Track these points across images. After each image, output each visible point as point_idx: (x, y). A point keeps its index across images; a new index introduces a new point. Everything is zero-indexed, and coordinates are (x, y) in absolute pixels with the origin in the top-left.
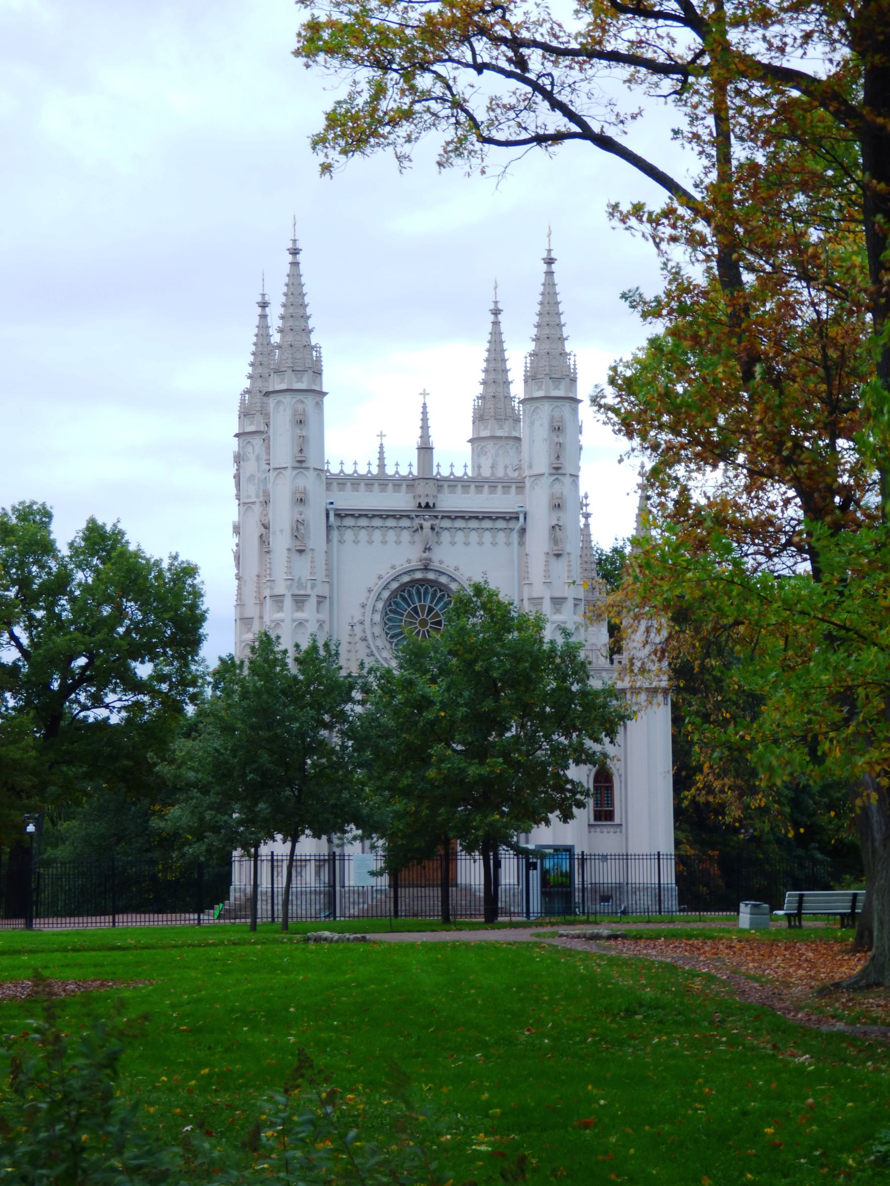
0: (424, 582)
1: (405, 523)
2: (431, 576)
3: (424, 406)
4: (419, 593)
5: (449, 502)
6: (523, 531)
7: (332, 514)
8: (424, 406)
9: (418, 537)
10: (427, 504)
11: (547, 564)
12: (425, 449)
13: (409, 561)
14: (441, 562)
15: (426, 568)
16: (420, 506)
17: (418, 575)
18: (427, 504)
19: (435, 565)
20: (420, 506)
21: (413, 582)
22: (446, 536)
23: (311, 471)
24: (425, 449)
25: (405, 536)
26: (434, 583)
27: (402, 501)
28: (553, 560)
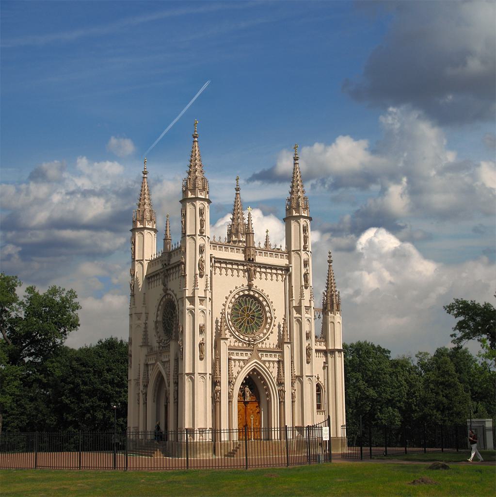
0: (248, 295)
1: (241, 267)
2: (252, 293)
4: (246, 301)
5: (259, 259)
6: (290, 276)
7: (213, 259)
14: (256, 287)
15: (249, 290)
16: (249, 260)
17: (246, 293)
19: (254, 288)
20: (249, 260)
21: (244, 295)
26: (253, 297)
27: (240, 257)
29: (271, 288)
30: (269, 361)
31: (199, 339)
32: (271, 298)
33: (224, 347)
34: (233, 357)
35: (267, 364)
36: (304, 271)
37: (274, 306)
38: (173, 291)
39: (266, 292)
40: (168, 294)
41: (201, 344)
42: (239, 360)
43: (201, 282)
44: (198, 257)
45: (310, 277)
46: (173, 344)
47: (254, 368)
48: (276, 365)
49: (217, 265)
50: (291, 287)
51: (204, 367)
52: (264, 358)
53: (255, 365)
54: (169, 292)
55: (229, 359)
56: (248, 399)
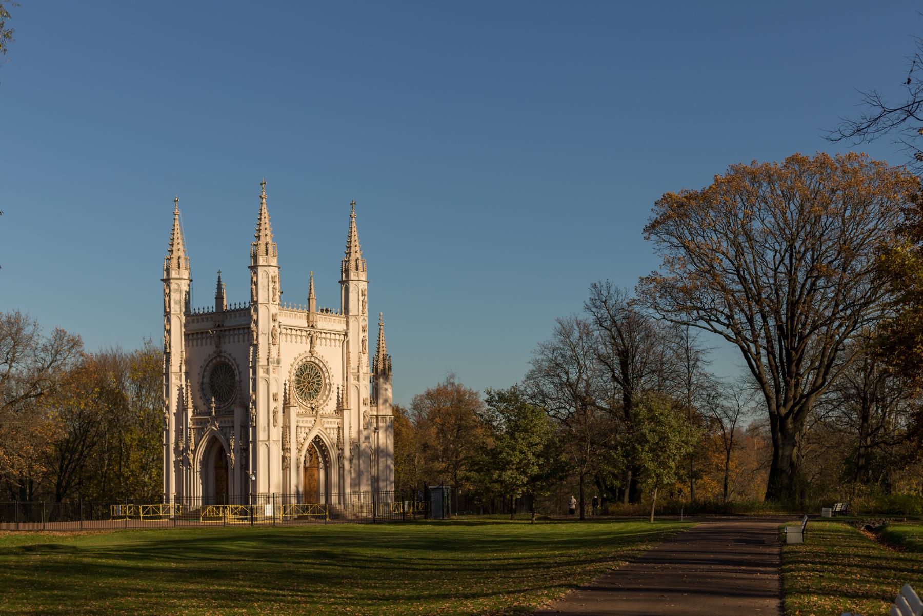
2: (313, 359)
6: (348, 342)
17: (308, 359)
29: (330, 354)
31: (273, 405)
32: (329, 365)
33: (293, 412)
34: (301, 424)
36: (362, 335)
37: (332, 372)
38: (230, 355)
39: (325, 359)
40: (221, 357)
41: (275, 413)
43: (274, 350)
44: (271, 327)
45: (367, 343)
46: (238, 412)
49: (284, 331)
50: (348, 353)
51: (276, 433)
52: (326, 425)
54: (222, 354)
56: (307, 465)
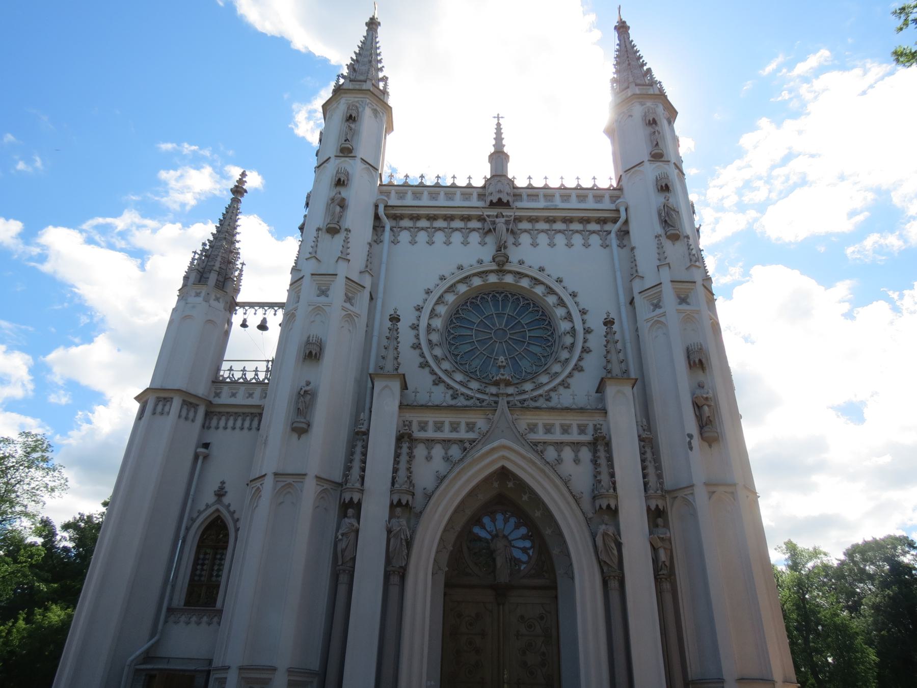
2: (509, 279)
3: (499, 125)
8: (499, 125)
9: (490, 239)
10: (500, 200)
11: (660, 246)
12: (499, 157)
13: (480, 262)
14: (521, 262)
17: (493, 278)
18: (500, 200)
22: (525, 239)
23: (358, 161)
24: (499, 157)
25: (475, 238)
28: (667, 244)
30: (559, 445)
35: (551, 454)
42: (446, 443)
47: (503, 468)
48: (585, 454)
53: (504, 457)
55: (400, 438)
